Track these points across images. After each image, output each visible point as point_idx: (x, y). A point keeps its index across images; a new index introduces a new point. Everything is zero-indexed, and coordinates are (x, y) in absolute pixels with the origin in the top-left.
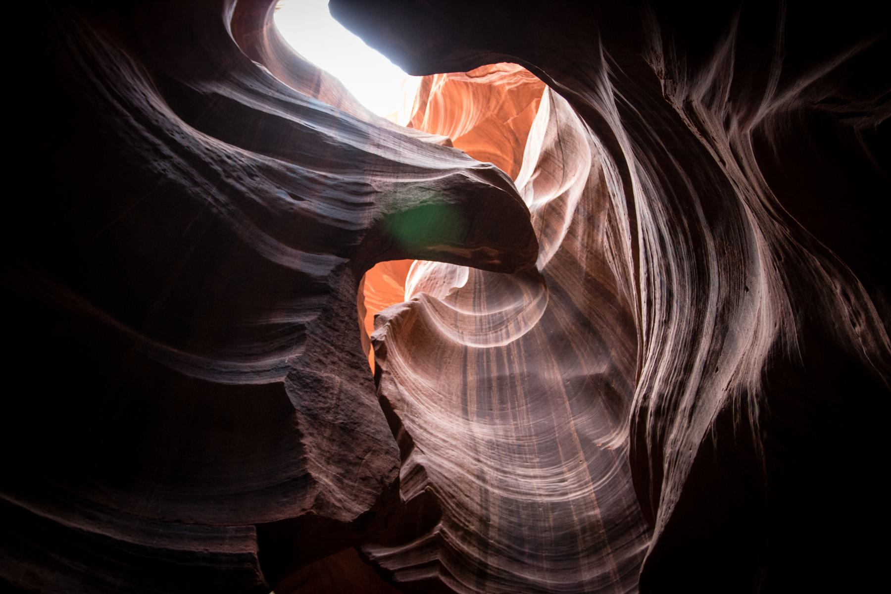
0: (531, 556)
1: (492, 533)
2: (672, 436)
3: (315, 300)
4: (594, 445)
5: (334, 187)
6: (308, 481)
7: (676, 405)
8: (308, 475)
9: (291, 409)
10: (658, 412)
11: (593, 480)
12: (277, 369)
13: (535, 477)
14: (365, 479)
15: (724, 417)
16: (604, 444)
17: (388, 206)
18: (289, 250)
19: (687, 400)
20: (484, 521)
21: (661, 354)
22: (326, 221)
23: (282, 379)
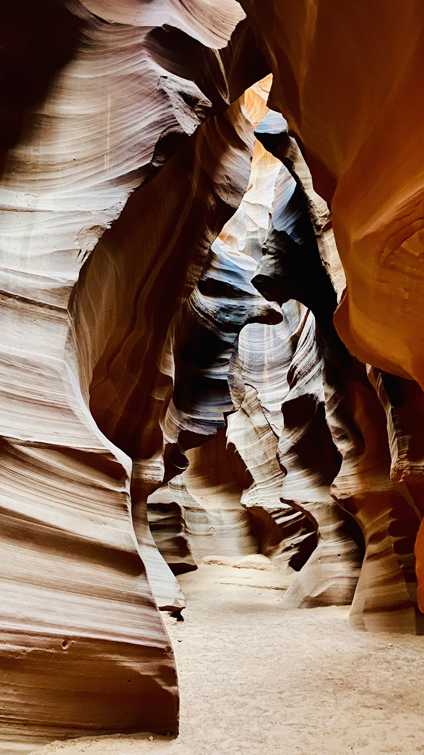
1: (244, 366)
3: (231, 350)
5: (236, 309)
6: (231, 403)
7: (304, 376)
10: (299, 373)
11: (274, 346)
12: (225, 374)
13: (256, 342)
14: (240, 399)
15: (312, 395)
16: (279, 335)
17: (249, 315)
18: (225, 334)
21: (304, 357)
22: (234, 323)
23: (226, 378)
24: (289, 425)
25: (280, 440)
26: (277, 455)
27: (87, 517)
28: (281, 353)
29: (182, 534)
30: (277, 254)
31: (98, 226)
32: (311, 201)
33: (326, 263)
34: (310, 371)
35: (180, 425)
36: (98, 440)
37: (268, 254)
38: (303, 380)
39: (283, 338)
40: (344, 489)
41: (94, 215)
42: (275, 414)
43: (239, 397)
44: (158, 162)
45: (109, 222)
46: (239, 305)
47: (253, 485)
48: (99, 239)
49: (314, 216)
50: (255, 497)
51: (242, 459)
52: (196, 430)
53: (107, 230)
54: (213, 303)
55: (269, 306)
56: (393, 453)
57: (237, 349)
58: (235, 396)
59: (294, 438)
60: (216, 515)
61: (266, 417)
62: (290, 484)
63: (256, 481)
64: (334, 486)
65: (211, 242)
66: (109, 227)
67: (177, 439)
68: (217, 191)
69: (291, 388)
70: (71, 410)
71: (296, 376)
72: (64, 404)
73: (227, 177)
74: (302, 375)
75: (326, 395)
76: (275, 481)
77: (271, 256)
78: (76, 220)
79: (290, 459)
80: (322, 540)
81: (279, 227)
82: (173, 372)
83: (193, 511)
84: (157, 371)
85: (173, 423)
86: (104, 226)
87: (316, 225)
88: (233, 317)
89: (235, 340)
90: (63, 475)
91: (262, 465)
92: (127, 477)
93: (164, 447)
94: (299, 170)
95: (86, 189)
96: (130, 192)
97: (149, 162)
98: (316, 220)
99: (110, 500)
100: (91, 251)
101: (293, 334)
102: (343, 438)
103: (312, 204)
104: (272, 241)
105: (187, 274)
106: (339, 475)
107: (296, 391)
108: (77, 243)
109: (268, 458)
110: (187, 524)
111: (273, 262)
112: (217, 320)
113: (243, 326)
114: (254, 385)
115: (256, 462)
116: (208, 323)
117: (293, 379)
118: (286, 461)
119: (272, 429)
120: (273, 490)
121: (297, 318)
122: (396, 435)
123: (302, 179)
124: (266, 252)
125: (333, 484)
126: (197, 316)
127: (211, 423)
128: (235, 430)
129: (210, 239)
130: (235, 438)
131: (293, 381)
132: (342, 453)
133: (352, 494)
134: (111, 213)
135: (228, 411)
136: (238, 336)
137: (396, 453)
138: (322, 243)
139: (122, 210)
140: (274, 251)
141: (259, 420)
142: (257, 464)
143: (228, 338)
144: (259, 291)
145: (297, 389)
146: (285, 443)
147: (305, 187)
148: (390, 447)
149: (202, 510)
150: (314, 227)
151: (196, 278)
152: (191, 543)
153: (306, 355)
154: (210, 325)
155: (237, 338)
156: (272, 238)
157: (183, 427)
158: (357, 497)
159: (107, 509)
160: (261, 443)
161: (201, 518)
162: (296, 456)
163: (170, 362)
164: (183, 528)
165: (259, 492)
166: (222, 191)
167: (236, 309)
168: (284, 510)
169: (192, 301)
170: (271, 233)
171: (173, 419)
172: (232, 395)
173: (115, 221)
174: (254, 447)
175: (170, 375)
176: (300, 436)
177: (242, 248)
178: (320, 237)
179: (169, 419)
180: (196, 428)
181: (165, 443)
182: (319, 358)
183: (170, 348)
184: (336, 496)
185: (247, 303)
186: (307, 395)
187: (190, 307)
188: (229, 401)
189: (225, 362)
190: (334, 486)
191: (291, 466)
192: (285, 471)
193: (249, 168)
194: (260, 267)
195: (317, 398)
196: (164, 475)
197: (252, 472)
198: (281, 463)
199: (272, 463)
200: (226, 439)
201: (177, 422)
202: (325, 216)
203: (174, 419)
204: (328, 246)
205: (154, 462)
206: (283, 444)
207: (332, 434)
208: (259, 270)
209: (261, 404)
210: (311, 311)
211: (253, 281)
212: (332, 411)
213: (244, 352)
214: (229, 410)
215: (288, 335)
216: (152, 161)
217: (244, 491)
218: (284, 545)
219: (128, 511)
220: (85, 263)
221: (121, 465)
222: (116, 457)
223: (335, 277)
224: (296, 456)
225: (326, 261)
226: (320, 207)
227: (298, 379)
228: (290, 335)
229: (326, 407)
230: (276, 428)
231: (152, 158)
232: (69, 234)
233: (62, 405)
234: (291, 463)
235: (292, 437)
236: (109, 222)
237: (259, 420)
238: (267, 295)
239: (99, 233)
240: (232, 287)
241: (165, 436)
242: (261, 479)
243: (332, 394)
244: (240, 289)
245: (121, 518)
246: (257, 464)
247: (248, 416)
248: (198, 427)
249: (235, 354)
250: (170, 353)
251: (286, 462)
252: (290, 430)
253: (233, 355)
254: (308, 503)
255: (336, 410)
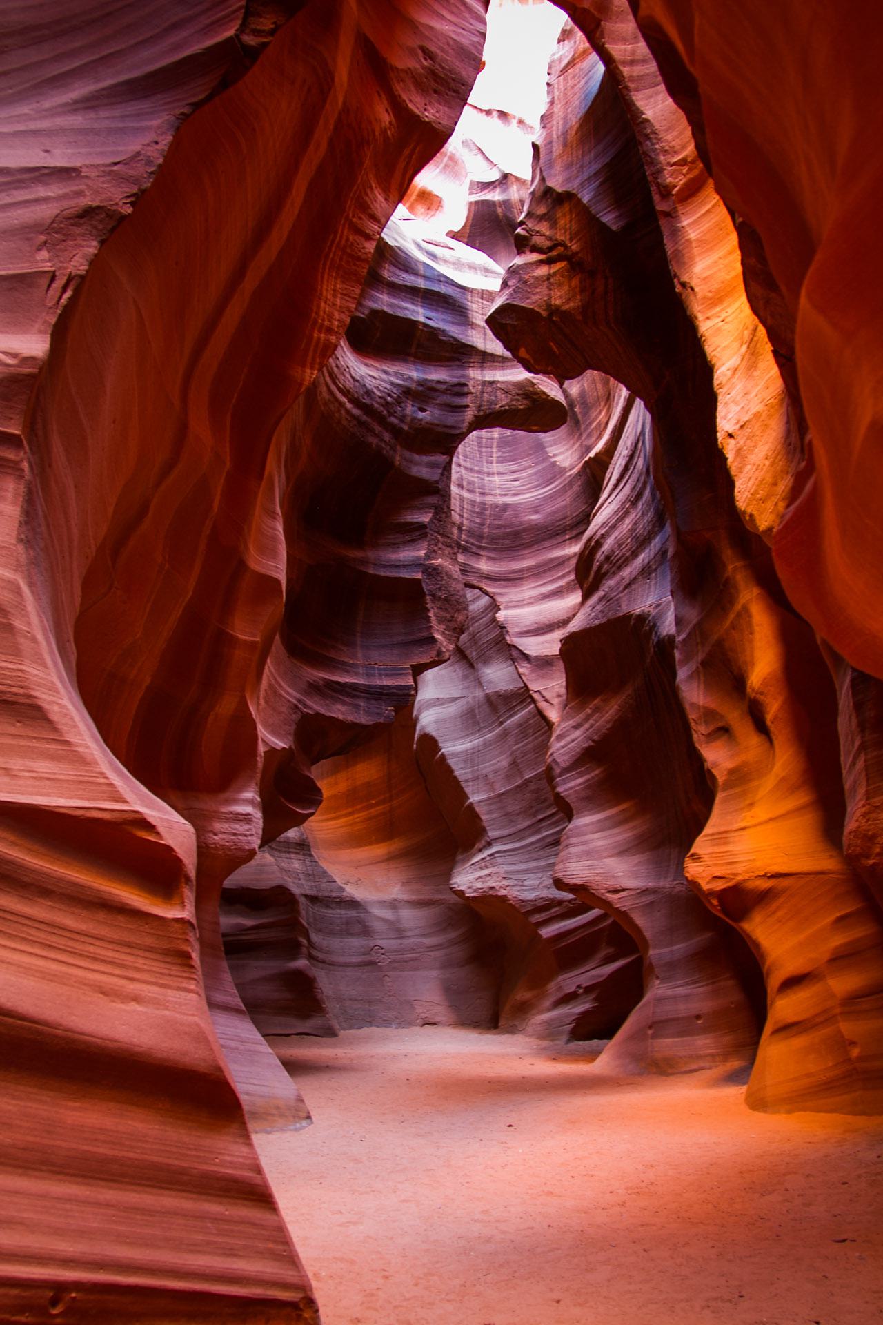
0: (485, 548)
2: (611, 583)
4: (546, 452)
5: (443, 392)
6: (432, 640)
7: (619, 568)
8: (433, 637)
9: (424, 595)
10: (607, 558)
12: (414, 564)
14: (454, 629)
15: (642, 618)
16: (554, 456)
18: (416, 457)
19: (627, 573)
20: (460, 528)
21: (621, 519)
22: (439, 429)
23: (419, 576)
24: (581, 689)
25: (557, 732)
26: (549, 769)
27: (90, 986)
28: (561, 503)
29: (301, 963)
30: (554, 253)
31: (98, 207)
32: (647, 120)
33: (684, 285)
34: (635, 554)
35: (299, 701)
36: (111, 785)
37: (532, 251)
38: (617, 578)
39: (567, 464)
40: (722, 865)
41: (87, 177)
42: (543, 663)
43: (452, 625)
44: (257, 33)
45: (127, 197)
46: (456, 380)
47: (483, 842)
48: (102, 243)
49: (652, 163)
50: (486, 872)
51: (455, 777)
52: (339, 711)
53: (123, 218)
54: (384, 376)
55: (533, 384)
56: (854, 789)
57: (446, 496)
58: (440, 621)
59: (591, 726)
60: (388, 914)
61: (521, 670)
62: (581, 844)
63: (492, 834)
64: (696, 857)
65: (383, 220)
66: (128, 210)
67: (291, 738)
68: (398, 88)
69: (585, 598)
70: (38, 708)
71: (600, 567)
72: (21, 691)
73: (423, 49)
74: (616, 563)
75: (679, 621)
76: (538, 832)
77: (535, 257)
78: (42, 192)
79: (580, 780)
80: (657, 982)
81: (557, 183)
82: (283, 566)
83: (328, 907)
84: (242, 565)
85: (280, 695)
86: (114, 208)
87: (658, 185)
88: (437, 412)
89: (442, 474)
90: (26, 879)
91: (507, 792)
92: (188, 879)
93: (260, 760)
94: (614, 41)
95: (66, 104)
96: (182, 114)
97: (231, 33)
98: (661, 171)
99: (149, 941)
100: (82, 277)
101: (592, 454)
102: (723, 731)
103: (649, 131)
104: (542, 218)
105: (319, 307)
106: (708, 830)
107: (599, 607)
108: (44, 254)
109: (521, 774)
110: (315, 938)
111: (543, 271)
112: (395, 421)
113: (462, 436)
114: (489, 586)
115: (491, 785)
116: (372, 431)
117: (592, 574)
118: (570, 786)
119: (534, 701)
120: (534, 855)
121: (600, 412)
122: (863, 747)
123: (624, 63)
124: (526, 245)
125: (692, 851)
126: (343, 412)
127: (381, 694)
128: (438, 702)
129: (379, 213)
130: (436, 722)
131: (590, 579)
132: (715, 772)
133: (740, 877)
134: (132, 173)
135: (422, 661)
136: (450, 463)
137: (862, 791)
138: (676, 232)
139: (161, 161)
140: (548, 244)
141: (498, 676)
142: (493, 790)
143: (422, 468)
144: (506, 347)
145: (601, 599)
146: (568, 739)
147: (632, 85)
148: (844, 772)
149: (353, 904)
150: (653, 189)
151: (343, 316)
152: (326, 984)
153: (627, 513)
154: (376, 436)
155: (447, 468)
156: (541, 210)
157: (306, 706)
158: (751, 885)
159: (140, 963)
160: (505, 734)
161: (347, 923)
162: (597, 772)
163: (274, 538)
164: (304, 950)
165: (499, 860)
166: (413, 89)
167: (443, 392)
168: (560, 902)
169: (331, 374)
170: (538, 194)
171: (281, 686)
172: (433, 618)
173: (143, 192)
174: (486, 745)
175: (274, 574)
176: (607, 722)
177: (458, 223)
178: (671, 215)
179: (270, 685)
180: (339, 707)
181: (262, 749)
182: (659, 521)
183: (274, 504)
184: (700, 881)
185: (476, 375)
186: (627, 617)
187: (324, 389)
188: (425, 634)
189: (417, 533)
190: (696, 857)
191: (583, 799)
192: (566, 811)
193: (480, 27)
194: (510, 283)
195: (655, 625)
196: (260, 832)
197: (481, 810)
198: (559, 789)
199: (532, 787)
200: (414, 722)
201: (291, 691)
202: (683, 162)
203: (285, 686)
204: (689, 241)
205: (236, 801)
206: (562, 743)
207: (693, 724)
208: (507, 292)
209: (507, 638)
210: (638, 401)
211: (491, 321)
212: (693, 665)
213: (462, 499)
214: (425, 659)
215: (576, 457)
216: (242, 29)
217: (459, 857)
218: (560, 988)
219: (193, 967)
220: (66, 307)
221: (169, 849)
222: (161, 829)
223: (709, 324)
224: (597, 772)
225: (684, 278)
226: (669, 137)
227: (605, 574)
228: (582, 457)
229: (677, 654)
230: (546, 701)
231: (239, 22)
232: (25, 231)
233: (16, 694)
234: (583, 789)
235: (587, 726)
236: (127, 197)
237: (498, 676)
238: (527, 357)
239: (101, 227)
240: (433, 334)
241: (262, 731)
242: (503, 827)
243: (694, 622)
244: (455, 339)
245: (175, 984)
246: (493, 790)
247: (472, 666)
248: (344, 703)
249: (442, 507)
250: (273, 516)
251: (571, 788)
252: (581, 707)
253: (436, 513)
254: (623, 890)
255: (702, 663)
